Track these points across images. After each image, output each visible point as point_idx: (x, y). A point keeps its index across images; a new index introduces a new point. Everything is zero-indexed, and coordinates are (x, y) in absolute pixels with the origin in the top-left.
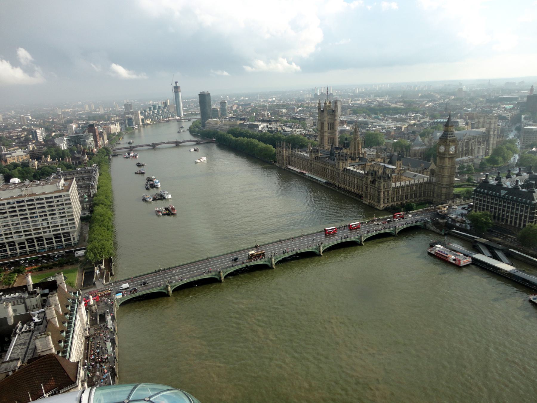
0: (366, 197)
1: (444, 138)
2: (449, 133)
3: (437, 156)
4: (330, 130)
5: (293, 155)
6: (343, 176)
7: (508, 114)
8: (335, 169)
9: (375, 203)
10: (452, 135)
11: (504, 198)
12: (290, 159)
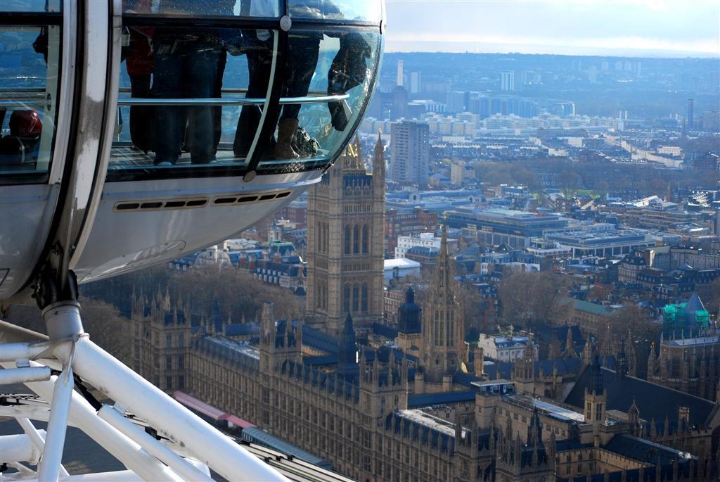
4: (352, 255)
6: (385, 445)
8: (354, 418)
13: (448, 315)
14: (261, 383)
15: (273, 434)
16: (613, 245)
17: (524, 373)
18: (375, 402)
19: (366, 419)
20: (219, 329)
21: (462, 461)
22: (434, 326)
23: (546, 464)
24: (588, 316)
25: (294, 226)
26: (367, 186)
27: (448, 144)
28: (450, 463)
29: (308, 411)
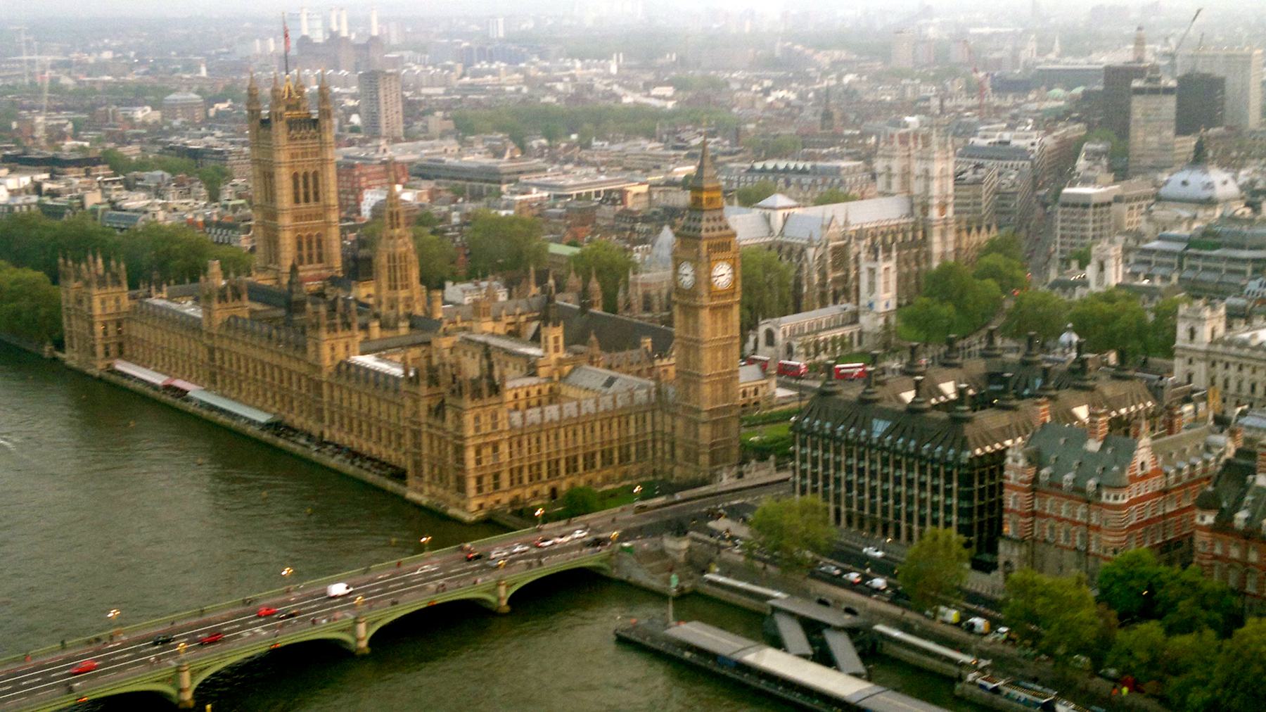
0: (419, 474)
2: (705, 216)
3: (675, 303)
4: (303, 205)
5: (133, 316)
6: (336, 394)
7: (1031, 137)
8: (304, 369)
10: (716, 225)
11: (883, 449)
12: (125, 332)
19: (318, 369)
20: (159, 290)
27: (429, 96)
29: (255, 367)
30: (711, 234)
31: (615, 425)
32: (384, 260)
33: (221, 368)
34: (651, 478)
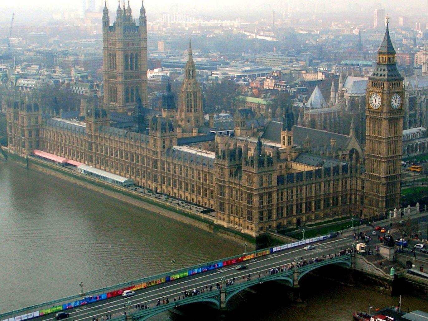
1: (379, 77)
3: (367, 116)
4: (130, 71)
9: (241, 221)
13: (194, 95)
14: (87, 140)
15: (96, 167)
16: (256, 73)
17: (240, 124)
18: (159, 142)
19: (155, 153)
20: (58, 113)
21: (220, 168)
22: (186, 101)
23: (271, 165)
24: (253, 105)
25: (83, 69)
26: (136, 31)
28: (209, 173)
29: (117, 152)
30: (391, 78)
31: (331, 186)
32: (185, 95)
33: (96, 154)
34: (348, 215)
